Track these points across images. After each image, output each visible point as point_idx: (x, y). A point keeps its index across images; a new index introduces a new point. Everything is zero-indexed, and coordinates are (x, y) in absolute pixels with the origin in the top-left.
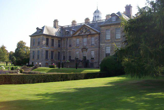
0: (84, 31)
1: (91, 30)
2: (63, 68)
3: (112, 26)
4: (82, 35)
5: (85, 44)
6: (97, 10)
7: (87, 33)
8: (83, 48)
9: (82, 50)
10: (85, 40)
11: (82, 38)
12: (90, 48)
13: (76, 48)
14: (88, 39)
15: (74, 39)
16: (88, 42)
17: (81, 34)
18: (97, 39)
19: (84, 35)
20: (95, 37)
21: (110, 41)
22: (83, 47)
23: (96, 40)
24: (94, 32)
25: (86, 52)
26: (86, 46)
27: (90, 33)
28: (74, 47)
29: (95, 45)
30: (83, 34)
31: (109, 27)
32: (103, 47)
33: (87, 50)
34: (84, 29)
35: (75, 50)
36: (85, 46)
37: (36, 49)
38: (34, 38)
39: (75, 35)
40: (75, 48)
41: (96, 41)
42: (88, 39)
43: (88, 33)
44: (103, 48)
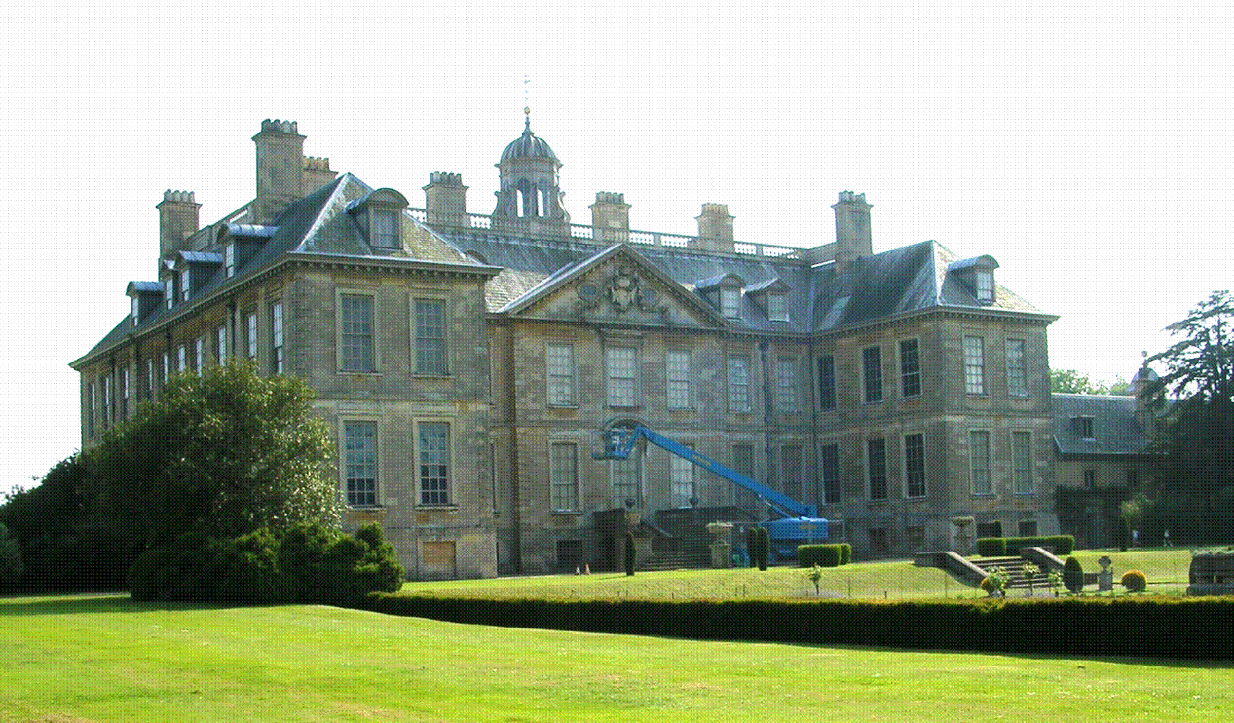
1: (666, 300)
2: (630, 573)
3: (991, 326)
5: (621, 395)
6: (527, 133)
7: (633, 316)
10: (621, 362)
13: (553, 417)
14: (648, 358)
15: (528, 343)
16: (650, 381)
18: (710, 364)
20: (697, 351)
21: (989, 404)
22: (609, 415)
23: (706, 374)
26: (637, 408)
28: (532, 406)
29: (700, 406)
30: (603, 313)
31: (978, 326)
32: (958, 435)
34: (625, 282)
35: (540, 431)
36: (627, 409)
37: (404, 407)
38: (363, 287)
39: (539, 315)
40: (545, 418)
41: (706, 383)
42: (648, 358)
44: (962, 441)
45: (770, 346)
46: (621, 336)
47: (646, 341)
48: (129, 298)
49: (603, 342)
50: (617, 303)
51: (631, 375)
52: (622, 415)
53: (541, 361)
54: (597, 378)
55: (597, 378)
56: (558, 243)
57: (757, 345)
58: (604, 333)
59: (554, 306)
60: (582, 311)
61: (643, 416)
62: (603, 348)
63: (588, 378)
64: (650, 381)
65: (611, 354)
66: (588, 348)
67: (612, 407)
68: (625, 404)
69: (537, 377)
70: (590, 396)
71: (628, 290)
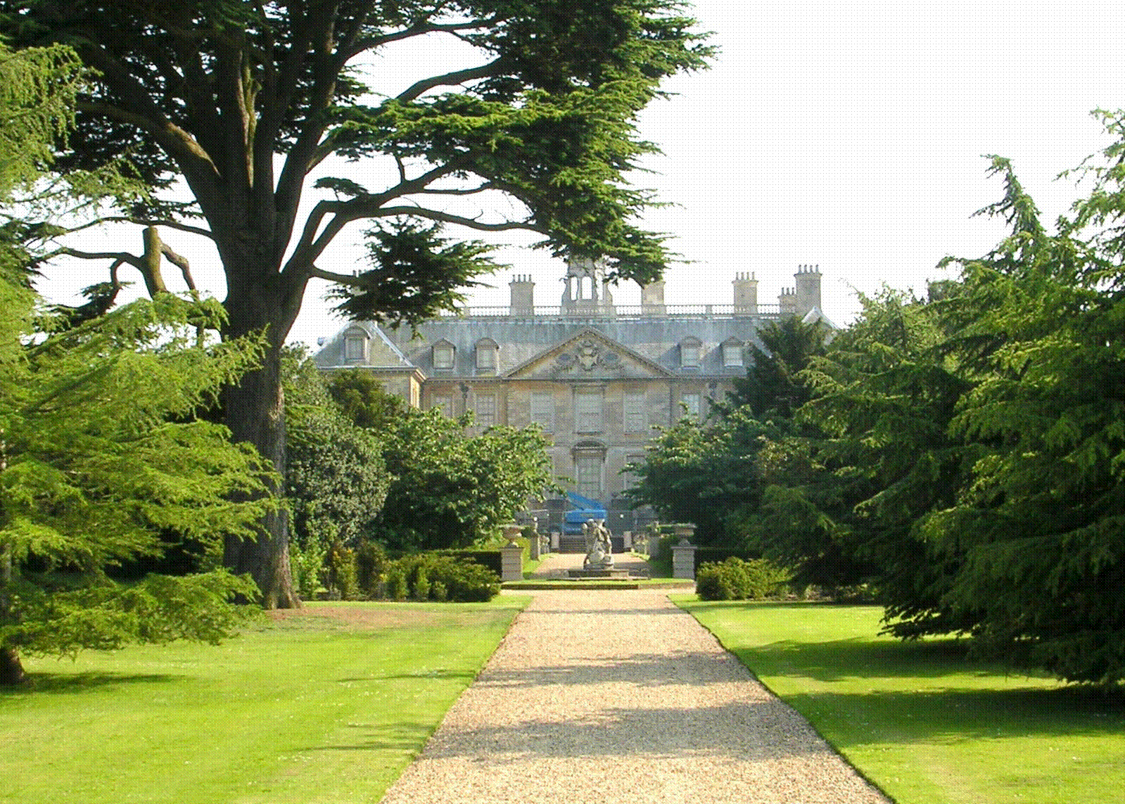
0: (588, 362)
1: (624, 360)
4: (573, 381)
7: (597, 373)
8: (579, 445)
9: (574, 451)
10: (589, 403)
11: (570, 390)
12: (622, 444)
14: (609, 400)
15: (518, 395)
16: (610, 414)
17: (564, 375)
19: (580, 381)
22: (577, 439)
23: (657, 408)
24: (640, 371)
25: (596, 461)
27: (617, 371)
30: (574, 372)
33: (605, 450)
36: (591, 434)
39: (527, 376)
41: (657, 414)
42: (609, 400)
43: (609, 374)
45: (719, 384)
46: (586, 386)
47: (607, 389)
48: (820, 271)
49: (574, 392)
50: (583, 365)
51: (596, 411)
52: (586, 438)
53: (527, 405)
54: (568, 414)
55: (568, 414)
56: (580, 320)
57: (707, 385)
58: (577, 385)
59: (538, 370)
60: (558, 371)
61: (602, 439)
62: (574, 393)
63: (562, 415)
64: (610, 414)
65: (582, 397)
66: (561, 396)
67: (579, 433)
68: (591, 430)
69: (523, 415)
70: (563, 426)
71: (592, 355)
